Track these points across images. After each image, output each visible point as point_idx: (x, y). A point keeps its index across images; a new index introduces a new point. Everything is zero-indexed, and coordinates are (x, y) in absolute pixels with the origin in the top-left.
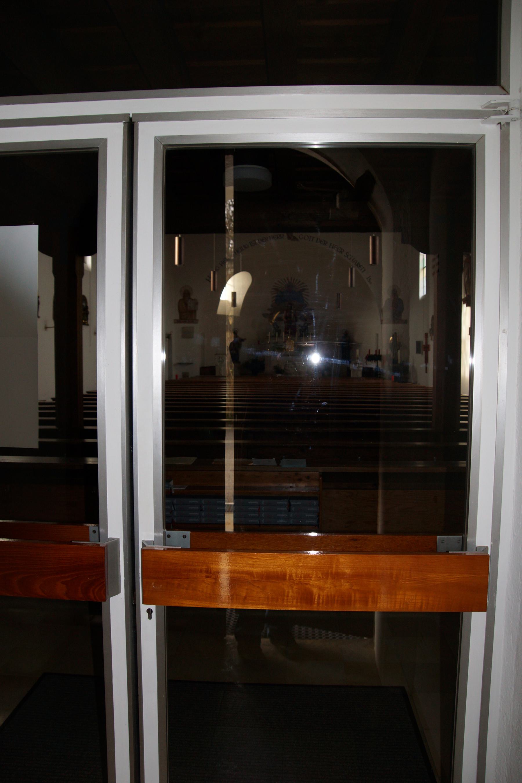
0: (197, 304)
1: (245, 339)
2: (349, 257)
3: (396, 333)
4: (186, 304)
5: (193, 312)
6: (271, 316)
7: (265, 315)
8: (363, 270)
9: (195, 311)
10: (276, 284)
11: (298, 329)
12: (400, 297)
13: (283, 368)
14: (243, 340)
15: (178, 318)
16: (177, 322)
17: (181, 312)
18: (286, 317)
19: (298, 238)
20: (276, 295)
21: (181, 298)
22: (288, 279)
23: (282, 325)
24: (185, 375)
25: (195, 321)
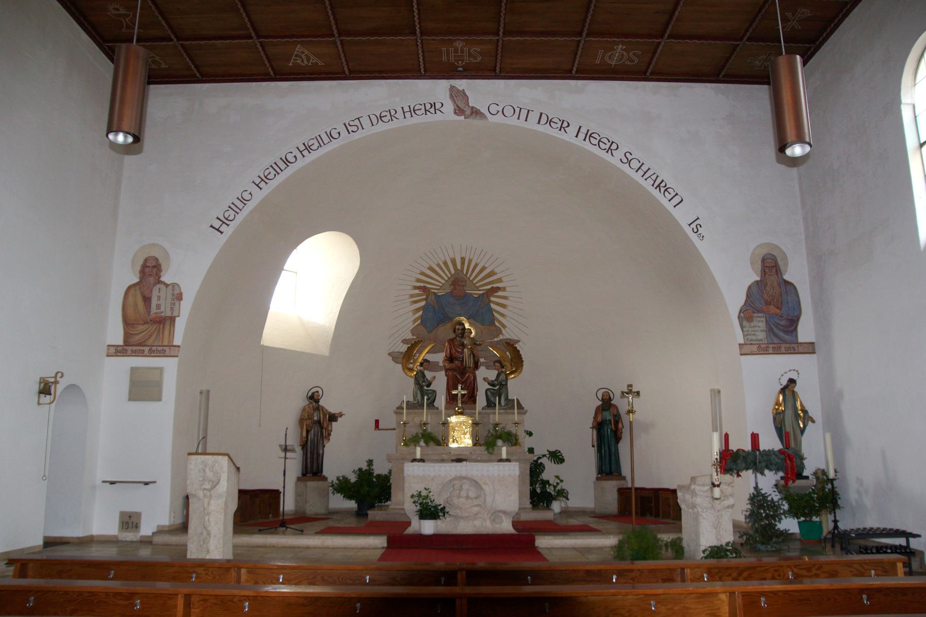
0: (180, 297)
1: (341, 415)
2: (635, 164)
3: (792, 381)
4: (147, 300)
5: (166, 322)
7: (394, 356)
8: (677, 200)
9: (172, 320)
10: (422, 274)
11: (482, 387)
12: (787, 277)
13: (439, 500)
14: (333, 418)
16: (118, 351)
18: (450, 359)
19: (484, 110)
20: (423, 303)
21: (136, 280)
23: (440, 382)
25: (165, 349)
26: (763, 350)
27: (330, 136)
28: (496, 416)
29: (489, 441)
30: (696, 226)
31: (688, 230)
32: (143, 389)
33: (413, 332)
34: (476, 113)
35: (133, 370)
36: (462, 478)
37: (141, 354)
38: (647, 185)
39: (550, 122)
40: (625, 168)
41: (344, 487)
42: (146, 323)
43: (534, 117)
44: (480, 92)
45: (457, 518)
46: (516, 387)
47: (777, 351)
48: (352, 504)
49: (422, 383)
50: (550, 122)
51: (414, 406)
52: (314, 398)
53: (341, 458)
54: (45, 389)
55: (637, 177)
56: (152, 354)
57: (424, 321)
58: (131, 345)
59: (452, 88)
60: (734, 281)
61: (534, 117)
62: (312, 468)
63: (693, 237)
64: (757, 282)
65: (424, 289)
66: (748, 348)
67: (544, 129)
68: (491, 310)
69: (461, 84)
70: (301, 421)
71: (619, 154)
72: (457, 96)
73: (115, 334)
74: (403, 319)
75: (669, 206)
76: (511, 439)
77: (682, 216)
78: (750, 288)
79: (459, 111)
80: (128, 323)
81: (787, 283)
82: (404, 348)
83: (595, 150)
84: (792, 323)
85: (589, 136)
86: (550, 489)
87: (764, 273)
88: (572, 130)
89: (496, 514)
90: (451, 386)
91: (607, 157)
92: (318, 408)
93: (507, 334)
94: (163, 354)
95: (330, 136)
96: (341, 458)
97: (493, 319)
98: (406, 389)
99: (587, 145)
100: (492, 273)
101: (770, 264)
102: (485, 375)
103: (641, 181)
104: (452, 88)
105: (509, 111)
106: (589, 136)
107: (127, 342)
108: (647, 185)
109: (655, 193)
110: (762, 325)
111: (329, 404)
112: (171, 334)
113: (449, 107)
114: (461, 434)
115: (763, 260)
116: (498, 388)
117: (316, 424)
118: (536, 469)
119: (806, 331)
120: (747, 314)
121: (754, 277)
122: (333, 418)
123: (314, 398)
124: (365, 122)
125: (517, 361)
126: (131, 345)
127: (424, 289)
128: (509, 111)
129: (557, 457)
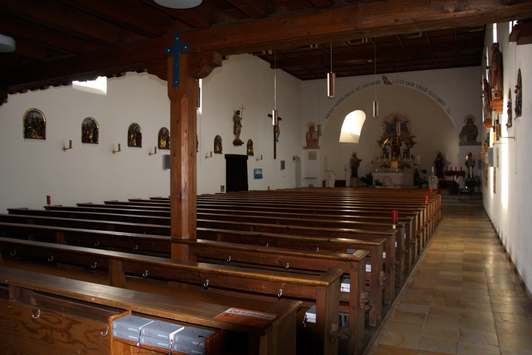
2: (432, 94)
4: (311, 135)
6: (381, 142)
9: (318, 140)
11: (402, 151)
12: (475, 124)
13: (381, 181)
14: (360, 161)
15: (306, 145)
16: (305, 148)
17: (307, 141)
21: (308, 131)
22: (394, 114)
24: (311, 187)
25: (317, 147)
26: (466, 144)
27: (353, 92)
28: (405, 160)
29: (402, 167)
30: (449, 111)
31: (446, 112)
32: (312, 157)
33: (384, 134)
34: (389, 83)
35: (309, 153)
36: (386, 177)
37: (311, 148)
38: (435, 100)
39: (409, 84)
40: (429, 96)
41: (363, 179)
42: (312, 141)
43: (405, 83)
44: (391, 77)
45: (385, 186)
46: (412, 151)
47: (470, 145)
48: (365, 184)
49: (385, 149)
50: (409, 84)
51: (382, 158)
52: (354, 155)
53: (362, 172)
54: (294, 159)
55: (432, 98)
56: (314, 148)
57: (387, 131)
58: (308, 146)
59: (383, 76)
60: (459, 125)
61: (405, 83)
62: (354, 174)
63: (448, 114)
64: (465, 126)
65: (386, 122)
66: (460, 144)
67: (408, 86)
68: (407, 128)
69: (385, 75)
70: (351, 162)
71: (428, 92)
72: (385, 78)
73: (305, 144)
74: (381, 131)
75: (441, 106)
76: (408, 166)
77: (445, 108)
78: (463, 128)
79: (385, 83)
80: (307, 141)
81: (475, 126)
82: (381, 139)
83: (422, 91)
84: (475, 137)
85: (420, 87)
86: (423, 181)
87: (468, 123)
88: (415, 86)
89: (395, 185)
90: (392, 152)
91: (425, 93)
92: (356, 158)
93: (412, 134)
94: (316, 148)
95: (353, 92)
96: (362, 172)
97: (408, 130)
98: (379, 152)
99: (419, 90)
100: (406, 117)
101: (470, 121)
102: (403, 147)
103: (434, 99)
104: (383, 76)
105: (398, 82)
106: (420, 87)
107: (308, 146)
108: (435, 100)
109: (438, 102)
110: (466, 138)
111: (359, 157)
112: (318, 144)
113: (382, 81)
114: (395, 165)
115: (468, 120)
116: (407, 152)
117: (355, 163)
118: (416, 175)
119: (478, 140)
120: (461, 135)
121: (464, 124)
122: (360, 161)
123: (354, 155)
124: (361, 87)
125: (412, 144)
126: (308, 146)
127: (386, 122)
128: (398, 82)
129: (424, 171)
